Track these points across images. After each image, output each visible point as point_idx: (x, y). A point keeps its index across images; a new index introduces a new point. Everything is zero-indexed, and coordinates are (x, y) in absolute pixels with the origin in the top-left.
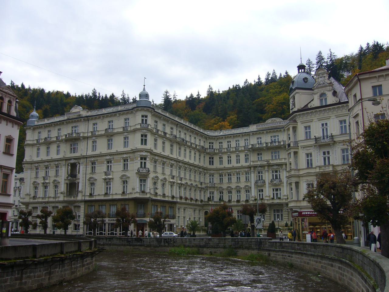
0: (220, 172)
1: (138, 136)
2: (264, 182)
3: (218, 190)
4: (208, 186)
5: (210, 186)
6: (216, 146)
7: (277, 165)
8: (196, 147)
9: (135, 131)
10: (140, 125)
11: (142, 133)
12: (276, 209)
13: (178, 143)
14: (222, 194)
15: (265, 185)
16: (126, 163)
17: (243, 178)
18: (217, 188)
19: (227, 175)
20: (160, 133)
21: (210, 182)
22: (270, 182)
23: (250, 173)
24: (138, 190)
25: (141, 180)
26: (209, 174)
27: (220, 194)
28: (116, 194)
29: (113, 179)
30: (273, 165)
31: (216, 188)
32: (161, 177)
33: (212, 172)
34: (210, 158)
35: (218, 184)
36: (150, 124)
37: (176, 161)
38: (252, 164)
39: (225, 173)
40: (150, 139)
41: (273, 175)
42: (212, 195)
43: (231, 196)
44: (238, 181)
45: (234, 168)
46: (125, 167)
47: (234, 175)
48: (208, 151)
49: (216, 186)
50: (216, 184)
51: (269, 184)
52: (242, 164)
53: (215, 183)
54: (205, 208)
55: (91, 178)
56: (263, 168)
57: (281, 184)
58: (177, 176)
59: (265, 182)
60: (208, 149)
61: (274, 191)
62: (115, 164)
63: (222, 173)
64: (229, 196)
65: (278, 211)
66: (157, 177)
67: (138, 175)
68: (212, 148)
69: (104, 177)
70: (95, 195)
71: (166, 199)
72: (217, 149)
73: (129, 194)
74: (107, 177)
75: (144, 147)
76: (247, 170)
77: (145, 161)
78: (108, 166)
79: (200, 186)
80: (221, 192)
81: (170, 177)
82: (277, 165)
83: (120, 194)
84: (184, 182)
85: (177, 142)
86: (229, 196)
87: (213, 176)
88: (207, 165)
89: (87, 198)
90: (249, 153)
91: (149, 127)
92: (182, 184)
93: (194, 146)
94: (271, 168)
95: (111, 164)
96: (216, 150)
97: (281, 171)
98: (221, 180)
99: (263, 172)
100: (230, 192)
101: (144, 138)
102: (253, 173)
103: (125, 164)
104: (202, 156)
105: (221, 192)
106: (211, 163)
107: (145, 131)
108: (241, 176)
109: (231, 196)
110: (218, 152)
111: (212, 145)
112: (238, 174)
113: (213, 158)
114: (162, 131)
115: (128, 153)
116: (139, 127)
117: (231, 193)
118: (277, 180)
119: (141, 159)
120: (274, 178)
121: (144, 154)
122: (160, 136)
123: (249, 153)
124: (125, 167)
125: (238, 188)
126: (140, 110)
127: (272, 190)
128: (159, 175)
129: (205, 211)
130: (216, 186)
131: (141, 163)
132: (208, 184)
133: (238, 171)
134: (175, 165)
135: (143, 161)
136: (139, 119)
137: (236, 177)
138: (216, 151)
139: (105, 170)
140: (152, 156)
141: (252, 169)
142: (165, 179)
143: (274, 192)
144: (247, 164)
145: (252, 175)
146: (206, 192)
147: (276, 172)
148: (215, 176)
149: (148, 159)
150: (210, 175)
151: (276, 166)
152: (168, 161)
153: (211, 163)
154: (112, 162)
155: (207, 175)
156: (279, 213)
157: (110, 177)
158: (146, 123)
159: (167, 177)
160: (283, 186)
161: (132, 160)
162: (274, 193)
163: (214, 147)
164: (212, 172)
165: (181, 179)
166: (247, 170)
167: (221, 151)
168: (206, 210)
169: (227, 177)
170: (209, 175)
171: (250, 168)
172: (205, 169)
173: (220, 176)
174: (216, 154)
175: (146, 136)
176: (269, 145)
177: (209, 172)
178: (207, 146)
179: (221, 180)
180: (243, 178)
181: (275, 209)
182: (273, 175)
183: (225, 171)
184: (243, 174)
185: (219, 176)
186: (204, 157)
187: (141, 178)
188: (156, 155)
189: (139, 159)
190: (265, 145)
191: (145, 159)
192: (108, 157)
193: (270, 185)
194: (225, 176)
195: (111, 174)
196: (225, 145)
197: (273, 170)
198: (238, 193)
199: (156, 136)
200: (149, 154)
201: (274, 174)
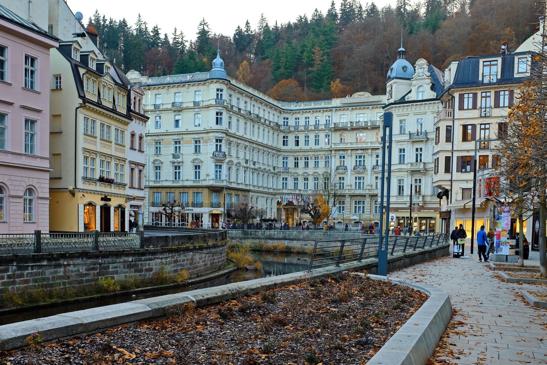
0: (296, 155)
1: (212, 114)
2: (346, 168)
4: (282, 171)
5: (284, 171)
6: (292, 122)
8: (270, 124)
9: (208, 107)
10: (215, 100)
11: (218, 111)
13: (252, 120)
14: (297, 181)
15: (347, 173)
16: (198, 144)
17: (322, 163)
19: (303, 158)
20: (234, 109)
22: (353, 169)
23: (330, 157)
24: (213, 176)
25: (216, 165)
27: (295, 181)
28: (187, 180)
29: (182, 162)
30: (358, 150)
31: (290, 174)
32: (235, 161)
33: (286, 154)
34: (284, 137)
36: (226, 100)
37: (250, 142)
39: (301, 156)
40: (225, 116)
41: (357, 161)
42: (285, 182)
43: (307, 183)
44: (315, 166)
45: (311, 150)
46: (197, 150)
47: (311, 159)
48: (282, 129)
49: (290, 171)
50: (290, 169)
52: (321, 146)
55: (155, 161)
56: (345, 152)
58: (251, 159)
59: (347, 169)
60: (282, 126)
61: (356, 180)
62: (185, 145)
64: (305, 183)
66: (232, 161)
67: (213, 160)
68: (287, 125)
69: (172, 160)
70: (162, 181)
71: (240, 187)
72: (292, 127)
73: (202, 180)
74: (175, 160)
75: (218, 127)
76: (326, 154)
77: (220, 144)
78: (176, 147)
79: (272, 171)
80: (296, 179)
81: (244, 161)
83: (191, 180)
84: (257, 166)
85: (251, 119)
86: (305, 183)
88: (280, 146)
89: (152, 184)
90: (330, 133)
91: (225, 104)
92: (255, 169)
93: (267, 123)
94: (355, 152)
95: (179, 145)
96: (291, 127)
97: (365, 156)
98: (296, 165)
99: (345, 157)
100: (306, 179)
101: (219, 116)
102: (334, 157)
103: (196, 146)
104: (276, 134)
105: (296, 179)
106: (285, 143)
107: (220, 108)
108: (319, 160)
109: (307, 183)
110: (293, 129)
111: (287, 121)
112: (316, 158)
113: (287, 137)
114: (236, 107)
115: (200, 133)
116: (213, 102)
117: (307, 180)
118: (360, 167)
119: (217, 141)
120: (358, 165)
121: (220, 135)
122: (234, 113)
123: (330, 133)
124: (197, 150)
125: (316, 174)
126: (215, 83)
127: (354, 178)
128: (233, 160)
130: (290, 171)
131: (217, 145)
132: (281, 169)
134: (249, 147)
135: (219, 144)
136: (213, 94)
137: (313, 161)
138: (291, 129)
139: (173, 151)
140: (228, 137)
141: (333, 152)
142: (239, 163)
144: (328, 147)
145: (333, 159)
146: (278, 179)
147: (360, 157)
148: (289, 159)
149: (223, 141)
150: (284, 158)
152: (242, 142)
153: (285, 143)
154: (181, 142)
155: (281, 158)
157: (180, 160)
158: (221, 99)
159: (241, 161)
160: (367, 174)
161: (206, 142)
162: (356, 182)
163: (289, 124)
165: (254, 163)
167: (298, 128)
169: (303, 161)
171: (331, 151)
172: (278, 151)
173: (295, 160)
174: (290, 132)
175: (221, 114)
176: (354, 125)
177: (283, 153)
178: (281, 122)
179: (296, 165)
180: (322, 163)
182: (357, 161)
183: (301, 154)
184: (322, 159)
185: (294, 159)
186: (278, 135)
187: (217, 164)
188: (231, 136)
189: (214, 141)
190: (349, 125)
191: (221, 141)
192: (176, 137)
193: (352, 173)
194: (301, 159)
195: (181, 157)
196: (302, 122)
197: (357, 155)
198: (315, 180)
199: (231, 113)
200: (224, 135)
201: (358, 160)
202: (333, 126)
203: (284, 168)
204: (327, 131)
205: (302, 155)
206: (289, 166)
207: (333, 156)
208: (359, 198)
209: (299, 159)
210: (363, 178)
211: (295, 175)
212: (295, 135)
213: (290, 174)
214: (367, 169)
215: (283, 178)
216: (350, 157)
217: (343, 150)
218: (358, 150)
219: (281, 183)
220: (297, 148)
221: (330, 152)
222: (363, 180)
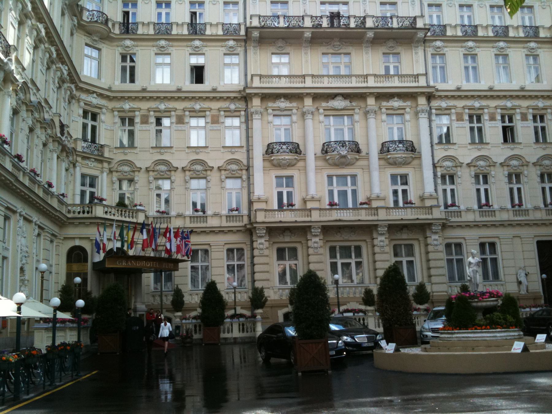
3: (114, 173)
7: (346, 96)
12: (338, 244)
18: (109, 163)
19: (153, 120)
21: (85, 140)
22: (319, 153)
26: (82, 104)
30: (333, 96)
31: (106, 165)
33: (94, 100)
35: (115, 151)
38: (256, 83)
51: (316, 158)
53: (102, 146)
54: (71, 231)
57: (357, 160)
63: (132, 110)
65: (346, 251)
82: (346, 96)
87: (94, 117)
94: (324, 104)
129: (70, 244)
130: (106, 155)
133: (197, 107)
141: (256, 102)
143: (331, 188)
145: (256, 124)
148: (103, 117)
151: (341, 98)
156: (350, 257)
164: (94, 100)
166: (233, 107)
168: (77, 243)
170: (81, 112)
181: (333, 244)
183: (144, 105)
193: (321, 163)
202: (255, 23)
203: (85, 145)
204: (231, 43)
205: (149, 110)
206: (102, 139)
207: (257, 113)
208: (346, 236)
209: (137, 120)
210: (354, 177)
211: (126, 168)
212: (120, 50)
213: (106, 165)
214: (363, 153)
215: (83, 176)
216: (310, 116)
217: (288, 97)
218: (333, 96)
219: (78, 192)
220: (128, 86)
221: (241, 105)
222: (354, 183)
